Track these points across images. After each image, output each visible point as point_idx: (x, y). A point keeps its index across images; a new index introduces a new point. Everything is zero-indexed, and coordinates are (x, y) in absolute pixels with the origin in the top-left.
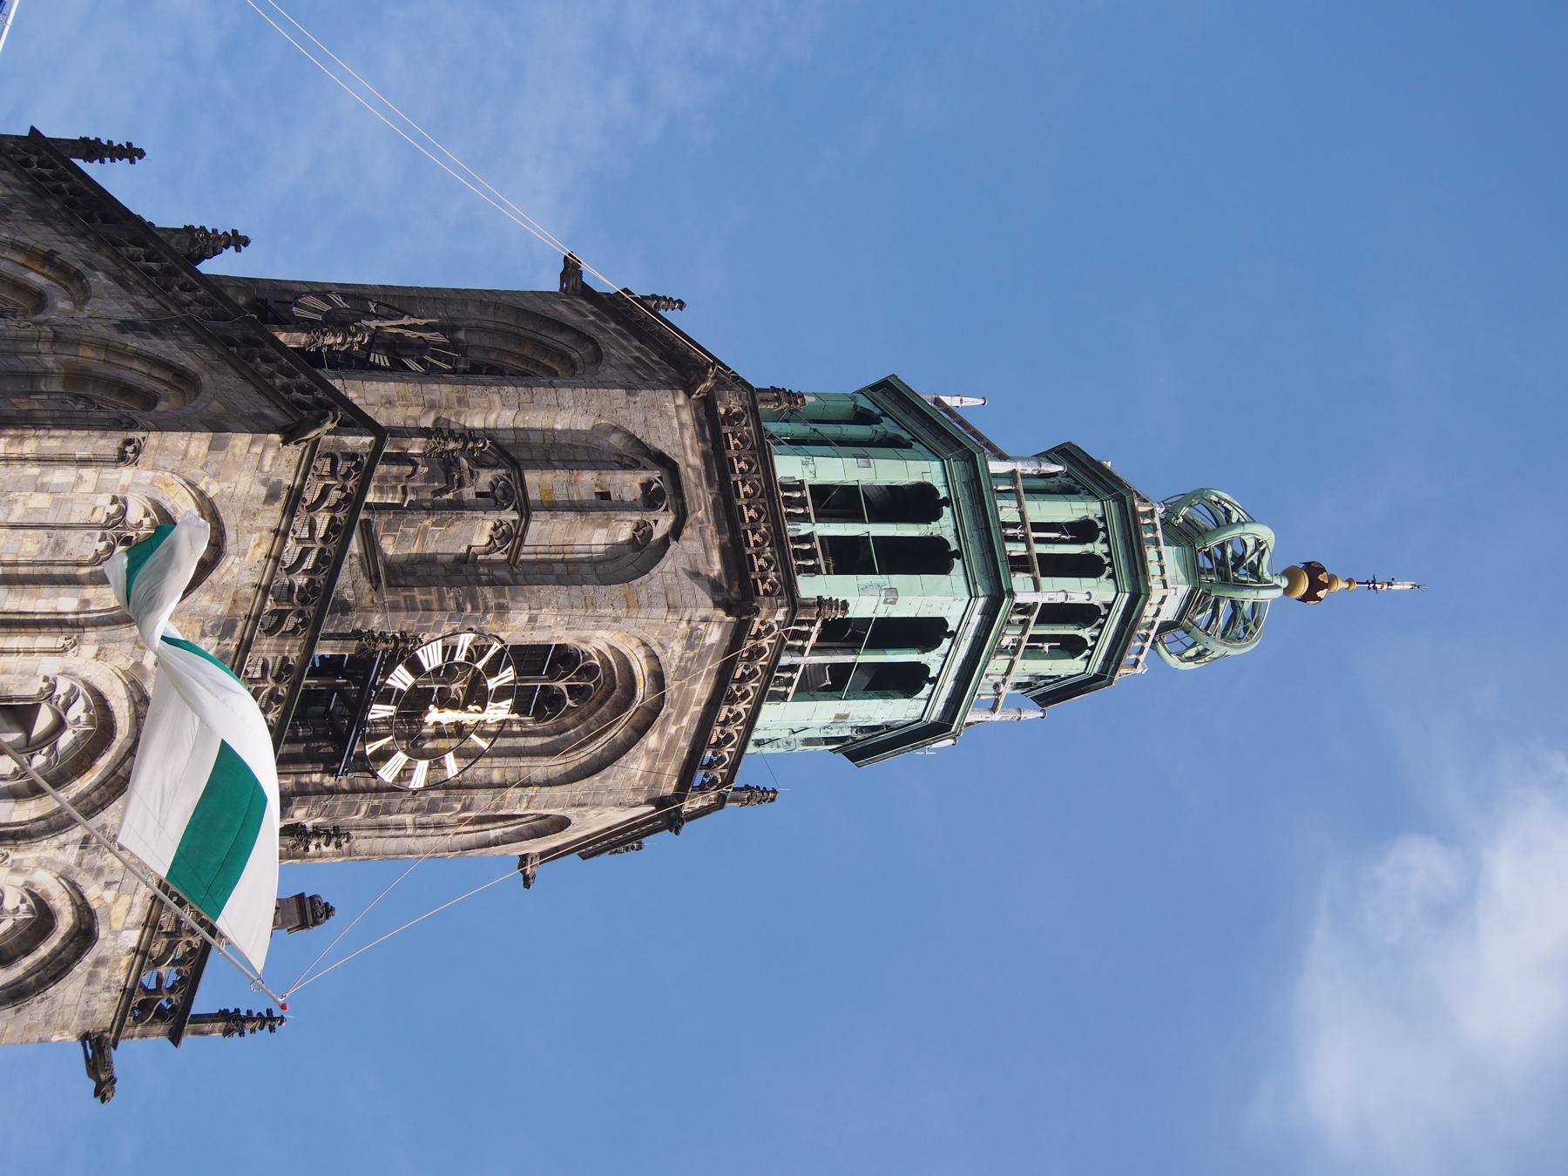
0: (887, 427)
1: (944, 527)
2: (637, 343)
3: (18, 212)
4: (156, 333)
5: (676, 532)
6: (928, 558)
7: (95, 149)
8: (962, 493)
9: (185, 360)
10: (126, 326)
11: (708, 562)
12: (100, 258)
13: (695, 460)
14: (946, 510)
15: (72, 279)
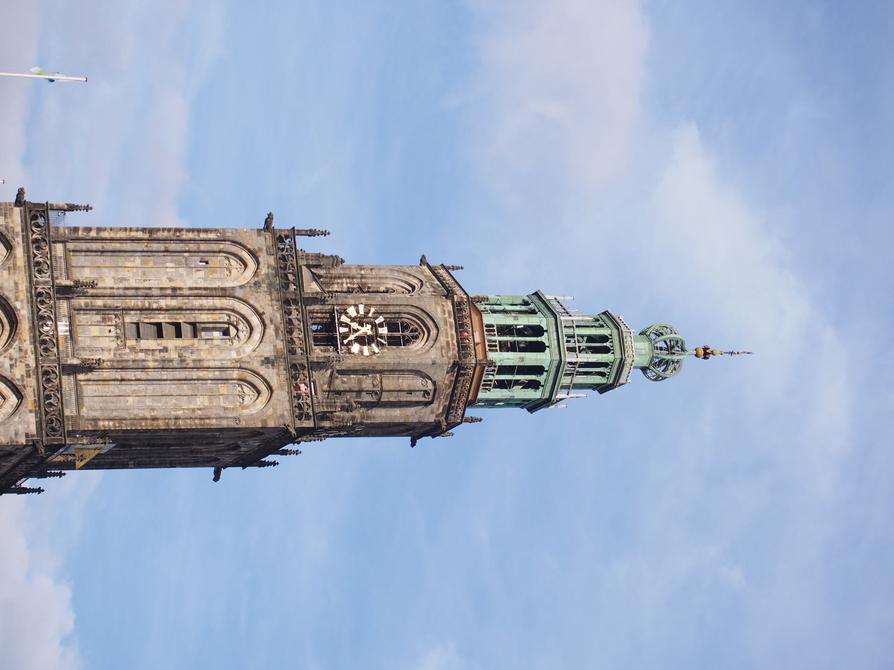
0: (543, 339)
1: (541, 378)
2: (454, 332)
3: (264, 287)
4: (273, 365)
5: (431, 402)
6: (535, 385)
7: (312, 233)
8: (553, 370)
9: (274, 383)
10: (267, 361)
11: (438, 409)
12: (278, 316)
13: (447, 382)
14: (545, 374)
15: (264, 325)
